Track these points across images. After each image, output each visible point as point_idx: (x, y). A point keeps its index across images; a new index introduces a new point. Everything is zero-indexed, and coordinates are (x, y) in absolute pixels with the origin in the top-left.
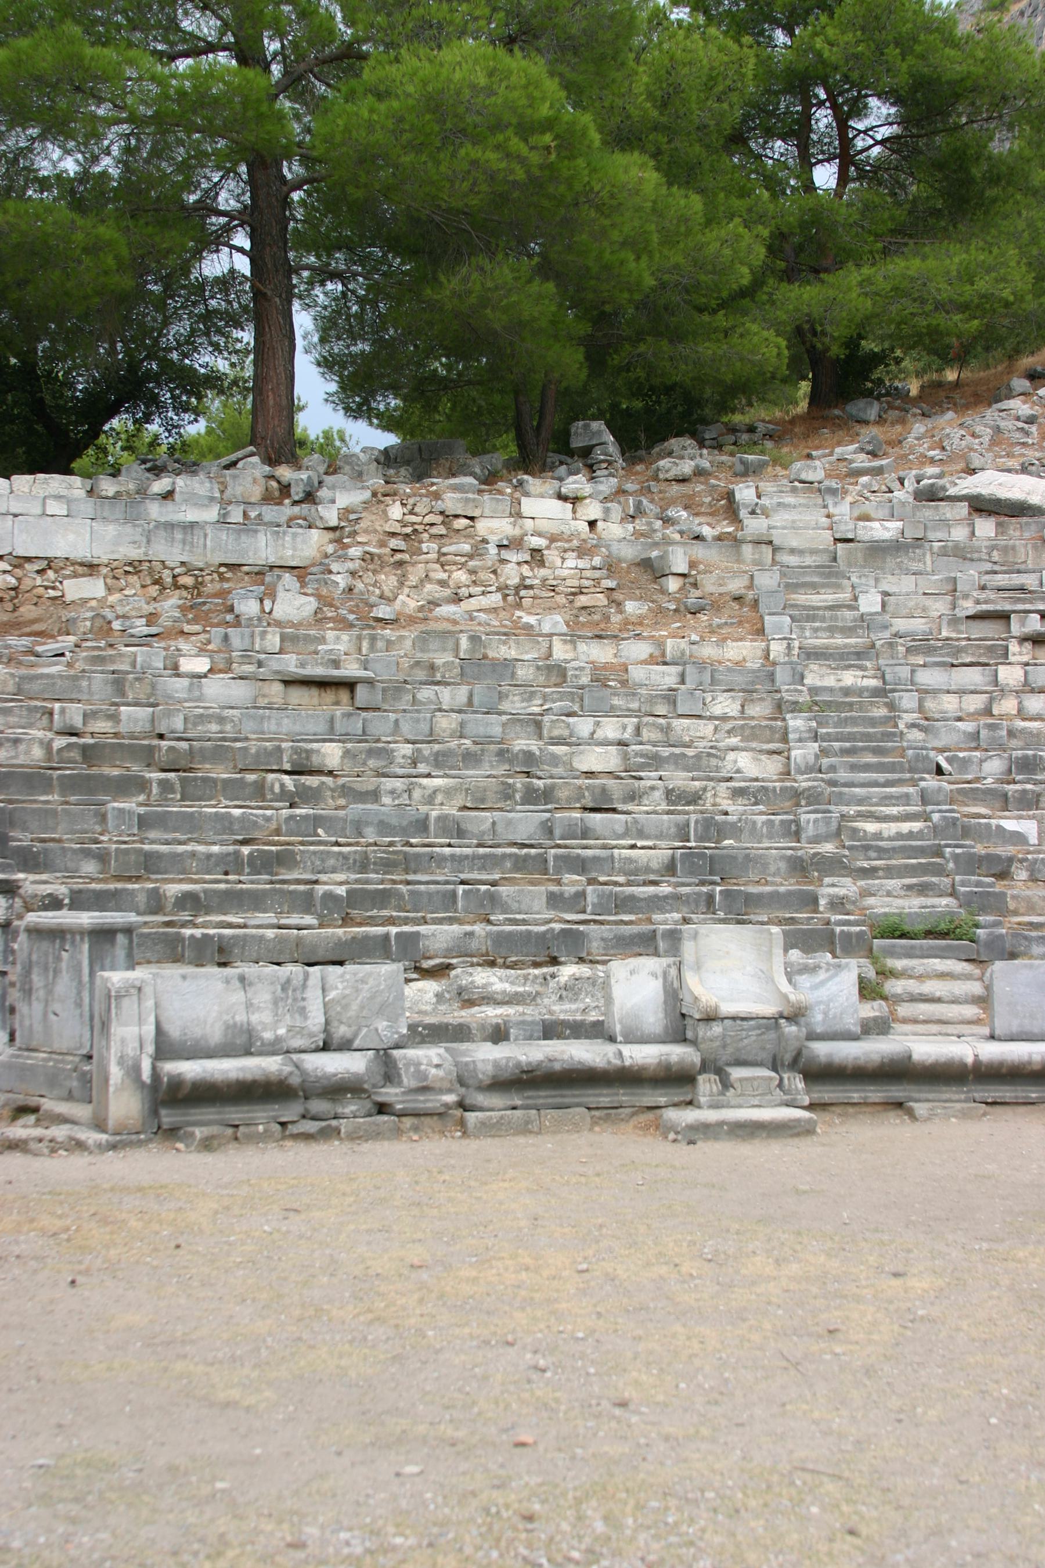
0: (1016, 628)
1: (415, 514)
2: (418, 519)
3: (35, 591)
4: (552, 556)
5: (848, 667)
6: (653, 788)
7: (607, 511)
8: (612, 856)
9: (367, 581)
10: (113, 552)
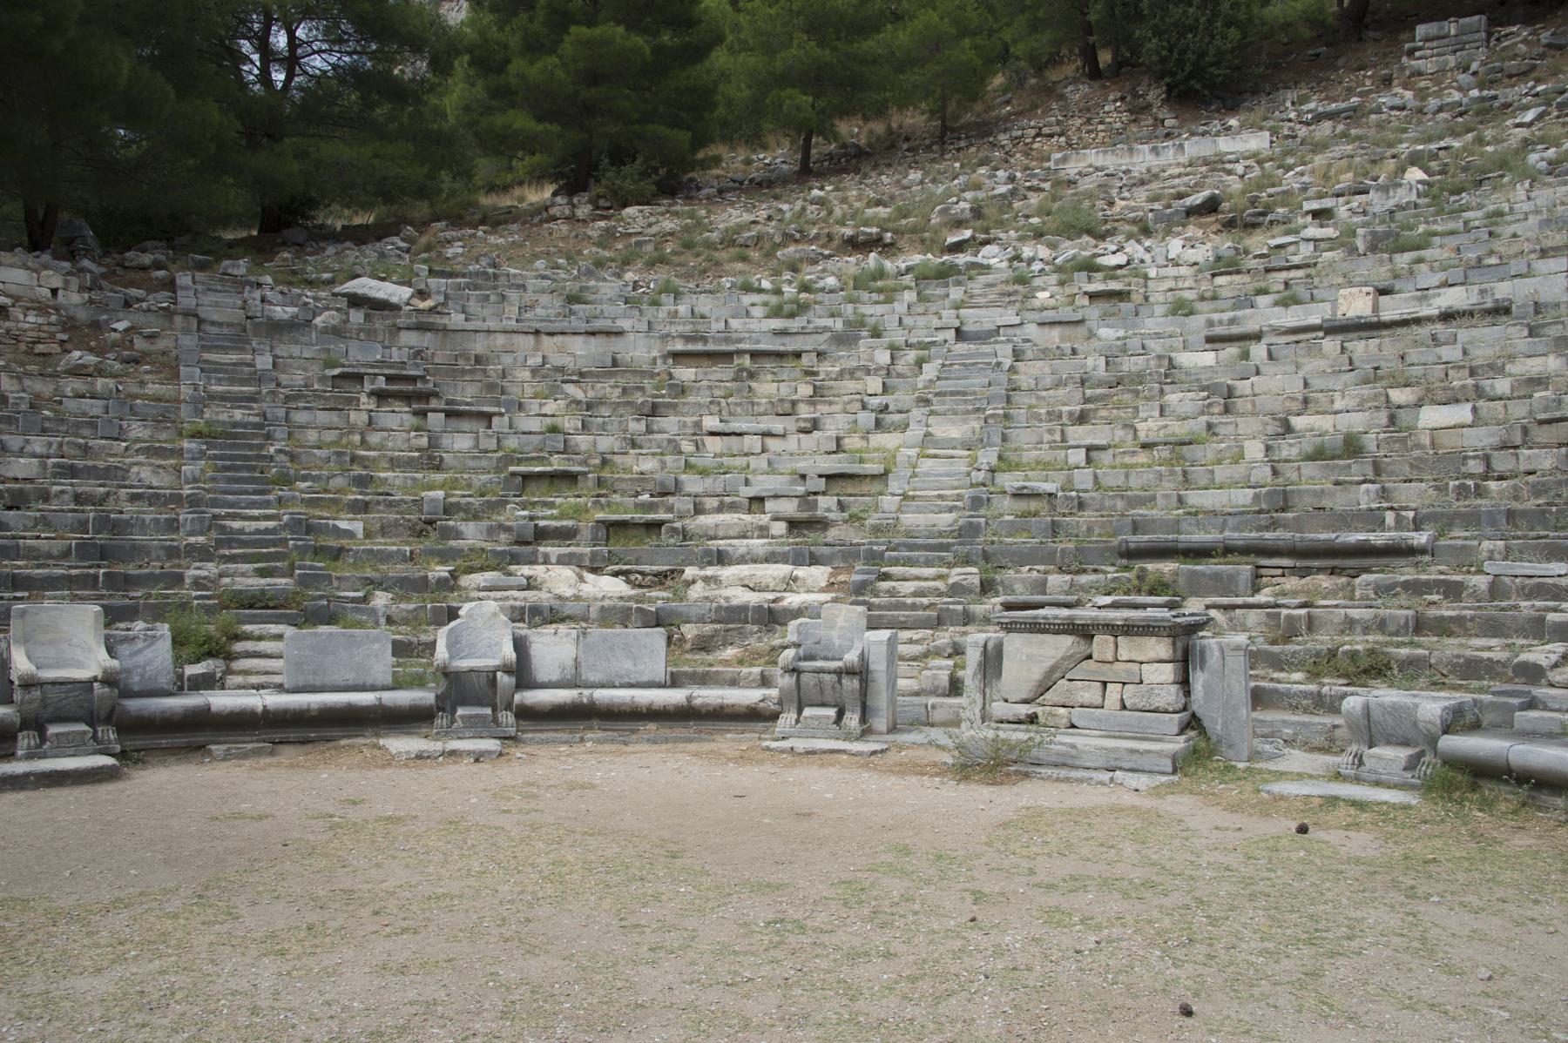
0: (368, 387)
4: (17, 312)
5: (239, 407)
6: (62, 492)
7: (67, 282)
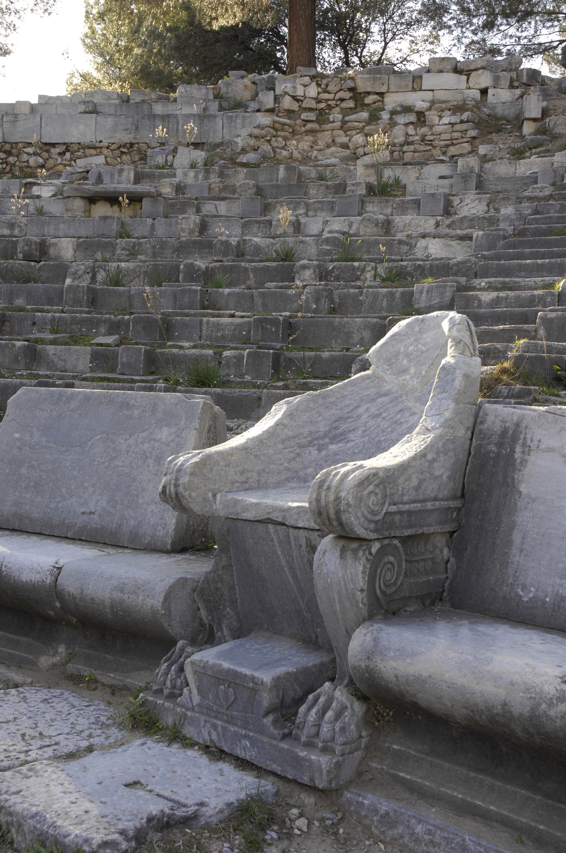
1: (329, 93)
2: (331, 96)
3: (56, 168)
4: (433, 117)
7: (496, 79)
8: (201, 322)
9: (275, 144)
10: (111, 137)
